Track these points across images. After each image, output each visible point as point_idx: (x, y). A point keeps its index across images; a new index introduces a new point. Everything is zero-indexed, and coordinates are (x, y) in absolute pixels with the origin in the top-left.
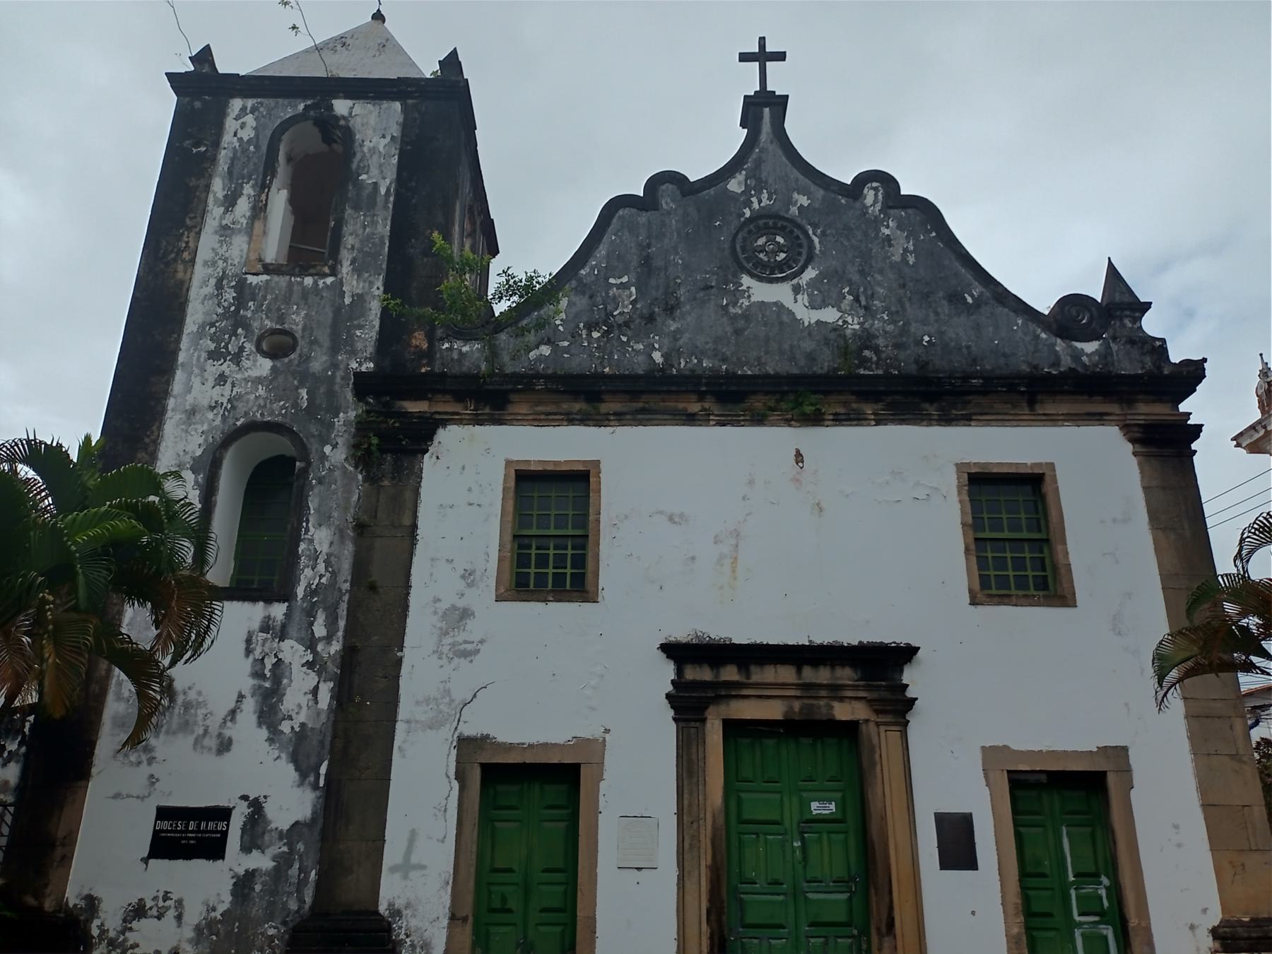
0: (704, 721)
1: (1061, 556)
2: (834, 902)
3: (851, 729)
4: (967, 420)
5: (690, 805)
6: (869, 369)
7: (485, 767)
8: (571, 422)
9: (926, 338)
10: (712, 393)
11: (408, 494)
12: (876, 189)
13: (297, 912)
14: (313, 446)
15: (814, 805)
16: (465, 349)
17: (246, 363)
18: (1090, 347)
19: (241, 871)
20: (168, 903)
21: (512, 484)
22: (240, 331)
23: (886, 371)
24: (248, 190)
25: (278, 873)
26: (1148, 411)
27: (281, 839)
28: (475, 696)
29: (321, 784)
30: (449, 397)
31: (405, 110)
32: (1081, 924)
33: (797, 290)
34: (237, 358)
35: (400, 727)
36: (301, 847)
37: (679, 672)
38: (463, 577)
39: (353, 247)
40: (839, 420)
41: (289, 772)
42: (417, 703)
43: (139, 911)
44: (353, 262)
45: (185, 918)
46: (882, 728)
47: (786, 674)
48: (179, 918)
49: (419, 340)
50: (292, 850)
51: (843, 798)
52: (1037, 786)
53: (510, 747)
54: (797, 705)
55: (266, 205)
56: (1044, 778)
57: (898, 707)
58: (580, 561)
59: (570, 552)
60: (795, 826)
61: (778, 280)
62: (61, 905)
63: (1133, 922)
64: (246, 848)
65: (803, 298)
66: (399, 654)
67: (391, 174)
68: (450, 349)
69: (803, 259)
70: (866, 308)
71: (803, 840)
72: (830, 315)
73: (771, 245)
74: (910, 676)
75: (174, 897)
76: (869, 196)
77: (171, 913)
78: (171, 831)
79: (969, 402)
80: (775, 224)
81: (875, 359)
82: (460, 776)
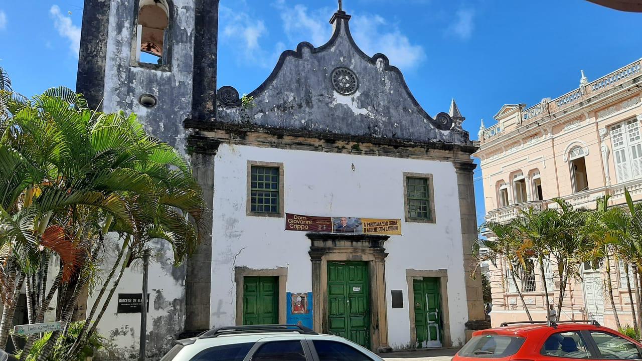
1: (432, 207)
2: (358, 321)
3: (367, 263)
7: (245, 277)
8: (272, 146)
9: (396, 124)
10: (324, 139)
11: (209, 172)
12: (381, 62)
13: (179, 331)
15: (354, 288)
16: (229, 111)
17: (135, 109)
18: (446, 133)
22: (131, 93)
23: (383, 136)
24: (127, 24)
25: (170, 318)
26: (463, 157)
29: (184, 284)
30: (223, 132)
32: (430, 324)
33: (353, 100)
34: (130, 105)
36: (178, 307)
37: (312, 244)
38: (234, 206)
39: (178, 59)
42: (219, 254)
44: (178, 66)
46: (377, 263)
47: (348, 243)
49: (209, 105)
50: (175, 309)
51: (363, 286)
52: (420, 281)
53: (254, 270)
55: (136, 33)
56: (422, 279)
57: (383, 255)
59: (271, 198)
60: (347, 295)
61: (346, 95)
63: (445, 322)
64: (157, 308)
65: (355, 103)
68: (223, 111)
69: (355, 89)
70: (376, 110)
71: (350, 300)
72: (364, 112)
74: (386, 245)
76: (379, 63)
78: (126, 303)
80: (346, 71)
81: (379, 130)
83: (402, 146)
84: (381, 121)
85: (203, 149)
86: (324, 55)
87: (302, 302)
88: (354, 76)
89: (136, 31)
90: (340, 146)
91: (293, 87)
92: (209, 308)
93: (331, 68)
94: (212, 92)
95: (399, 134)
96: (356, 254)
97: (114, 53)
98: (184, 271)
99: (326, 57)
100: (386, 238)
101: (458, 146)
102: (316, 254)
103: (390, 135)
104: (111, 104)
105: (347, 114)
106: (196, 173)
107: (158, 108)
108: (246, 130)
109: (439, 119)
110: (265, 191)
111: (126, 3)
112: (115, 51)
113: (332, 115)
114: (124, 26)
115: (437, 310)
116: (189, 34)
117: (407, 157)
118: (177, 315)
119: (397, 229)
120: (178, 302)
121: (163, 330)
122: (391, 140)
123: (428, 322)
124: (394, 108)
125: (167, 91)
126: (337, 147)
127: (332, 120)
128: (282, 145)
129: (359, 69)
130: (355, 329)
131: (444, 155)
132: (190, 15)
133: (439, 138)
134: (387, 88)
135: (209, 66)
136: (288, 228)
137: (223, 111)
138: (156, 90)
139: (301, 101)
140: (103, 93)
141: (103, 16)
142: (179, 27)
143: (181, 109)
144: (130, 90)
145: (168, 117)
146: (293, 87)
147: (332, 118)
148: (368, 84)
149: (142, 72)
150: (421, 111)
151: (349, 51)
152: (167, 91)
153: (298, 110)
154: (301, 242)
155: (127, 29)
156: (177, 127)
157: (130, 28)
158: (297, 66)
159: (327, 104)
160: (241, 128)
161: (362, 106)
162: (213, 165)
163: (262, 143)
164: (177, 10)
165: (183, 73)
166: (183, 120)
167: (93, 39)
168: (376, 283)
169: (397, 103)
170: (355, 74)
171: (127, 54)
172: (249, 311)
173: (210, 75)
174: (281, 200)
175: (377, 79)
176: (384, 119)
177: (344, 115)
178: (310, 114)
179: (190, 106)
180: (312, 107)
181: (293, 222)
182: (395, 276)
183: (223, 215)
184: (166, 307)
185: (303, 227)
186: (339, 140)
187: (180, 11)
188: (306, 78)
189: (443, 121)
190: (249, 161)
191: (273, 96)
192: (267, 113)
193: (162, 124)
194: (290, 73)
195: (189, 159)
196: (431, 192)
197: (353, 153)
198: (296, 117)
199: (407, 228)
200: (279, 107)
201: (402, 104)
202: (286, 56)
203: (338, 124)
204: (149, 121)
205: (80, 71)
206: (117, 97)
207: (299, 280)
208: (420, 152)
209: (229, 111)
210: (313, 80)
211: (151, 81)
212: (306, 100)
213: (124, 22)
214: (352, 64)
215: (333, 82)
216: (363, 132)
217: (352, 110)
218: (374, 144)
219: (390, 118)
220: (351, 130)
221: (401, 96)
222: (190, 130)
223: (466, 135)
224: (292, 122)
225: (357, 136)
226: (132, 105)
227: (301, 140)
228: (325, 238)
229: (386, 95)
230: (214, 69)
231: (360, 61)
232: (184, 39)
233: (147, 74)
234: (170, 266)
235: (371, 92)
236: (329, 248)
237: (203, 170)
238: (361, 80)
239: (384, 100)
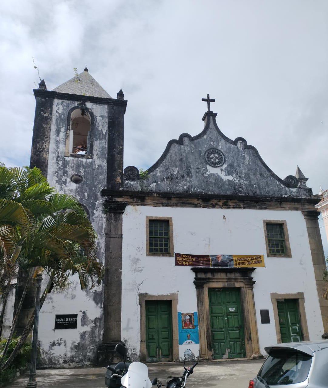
0: (203, 288)
3: (239, 289)
4: (265, 208)
5: (201, 310)
8: (163, 206)
9: (255, 186)
10: (202, 199)
11: (119, 225)
12: (241, 143)
13: (99, 342)
14: (90, 210)
17: (68, 184)
18: (294, 190)
19: (82, 332)
20: (62, 341)
21: (148, 223)
22: (65, 175)
24: (63, 130)
25: (93, 332)
26: (308, 207)
27: (92, 322)
28: (142, 282)
30: (128, 197)
31: (109, 109)
32: (292, 336)
33: (222, 170)
34: (65, 183)
35: (123, 291)
36: (98, 324)
37: (196, 275)
39: (97, 150)
40: (234, 207)
41: (93, 303)
43: (53, 344)
44: (97, 154)
45: (67, 345)
46: (247, 289)
47: (223, 275)
48: (65, 345)
49: (119, 180)
50: (96, 325)
51: (237, 307)
52: (282, 302)
53: (153, 296)
54: (226, 284)
55: (69, 135)
56: (283, 300)
57: (251, 283)
58: (167, 245)
59: (164, 242)
61: (217, 167)
64: (83, 325)
65: (223, 173)
66: (121, 271)
68: (128, 183)
69: (223, 162)
70: (240, 176)
71: (228, 318)
72: (230, 178)
73: (214, 157)
74: (254, 275)
75: (63, 339)
76: (240, 145)
77: (63, 344)
79: (266, 203)
80: (215, 151)
81: (242, 191)
82: (140, 304)
83: (261, 201)
84: (244, 184)
85: (115, 210)
86: (199, 141)
87: (190, 320)
88: (221, 154)
89: (69, 133)
90: (214, 203)
91: (177, 164)
92: (120, 325)
93: (204, 150)
94: (120, 171)
95: (258, 192)
96: (230, 283)
97: (54, 148)
98: (102, 297)
99: (201, 143)
100: (253, 270)
101: (304, 199)
102: (199, 284)
103: (251, 194)
104: (52, 182)
105: (218, 180)
106: (110, 227)
107: (84, 183)
108: (144, 195)
109: (288, 180)
110: (159, 239)
111: (62, 116)
112: (55, 147)
113: (206, 181)
114: (60, 131)
115: (298, 325)
116: (104, 134)
117: (265, 208)
118: (97, 329)
119: (260, 262)
120: (98, 320)
121: (87, 342)
122: (251, 197)
123: (292, 334)
124: (253, 174)
125: (89, 172)
126: (212, 204)
127: (207, 185)
128: (171, 205)
129: (225, 149)
130: (233, 340)
132: (105, 121)
134: (247, 161)
135: (118, 154)
136: (177, 264)
137: (128, 183)
138: (82, 171)
139: (184, 173)
140: (47, 175)
141: (47, 125)
142: (97, 129)
143: (99, 183)
144: (65, 173)
145: (90, 189)
146: (177, 164)
147: (207, 183)
148: (232, 158)
149: (73, 160)
150: (273, 175)
152: (89, 172)
153: (181, 179)
154: (187, 275)
155: (63, 133)
156: (96, 195)
157: (65, 132)
158: (180, 150)
159: (203, 174)
160: (141, 194)
162: (122, 220)
163: (156, 204)
164: (96, 118)
165: (101, 159)
166: (101, 190)
167: (40, 140)
168: (247, 305)
169: (255, 171)
170: (222, 152)
171: (63, 149)
172: (151, 326)
173: (119, 160)
174: (171, 243)
175: (239, 155)
176: (246, 182)
177: (215, 181)
178: (190, 182)
179: (105, 181)
180: (192, 177)
181: (181, 260)
182: (262, 298)
183: (130, 256)
184: (89, 324)
185: (188, 263)
186: (212, 199)
188: (187, 158)
189: (290, 182)
190: (147, 217)
191: (163, 171)
192: (159, 183)
193: (86, 194)
194: (175, 155)
195: (105, 217)
196: (286, 234)
197: (224, 207)
198: (180, 184)
199: (269, 261)
200: (167, 178)
201: (259, 172)
202: (172, 144)
203: (211, 188)
204: (78, 192)
205: (32, 161)
206: (56, 178)
207: (187, 303)
208: (275, 205)
209: (132, 183)
210: (191, 158)
211: (79, 166)
212: (187, 172)
213: (61, 129)
214: (220, 146)
215: (206, 159)
216: (231, 192)
217: (221, 178)
218: (239, 200)
219: (250, 181)
220: (221, 191)
221: (257, 165)
222: (106, 197)
223: (310, 191)
224: (177, 188)
225: (226, 195)
226: (66, 182)
228: (206, 271)
229: (246, 165)
230: (121, 155)
232: (101, 137)
233: (76, 161)
234: (92, 293)
235: (235, 164)
236: (209, 278)
237: (115, 224)
238: (227, 156)
239: (245, 169)
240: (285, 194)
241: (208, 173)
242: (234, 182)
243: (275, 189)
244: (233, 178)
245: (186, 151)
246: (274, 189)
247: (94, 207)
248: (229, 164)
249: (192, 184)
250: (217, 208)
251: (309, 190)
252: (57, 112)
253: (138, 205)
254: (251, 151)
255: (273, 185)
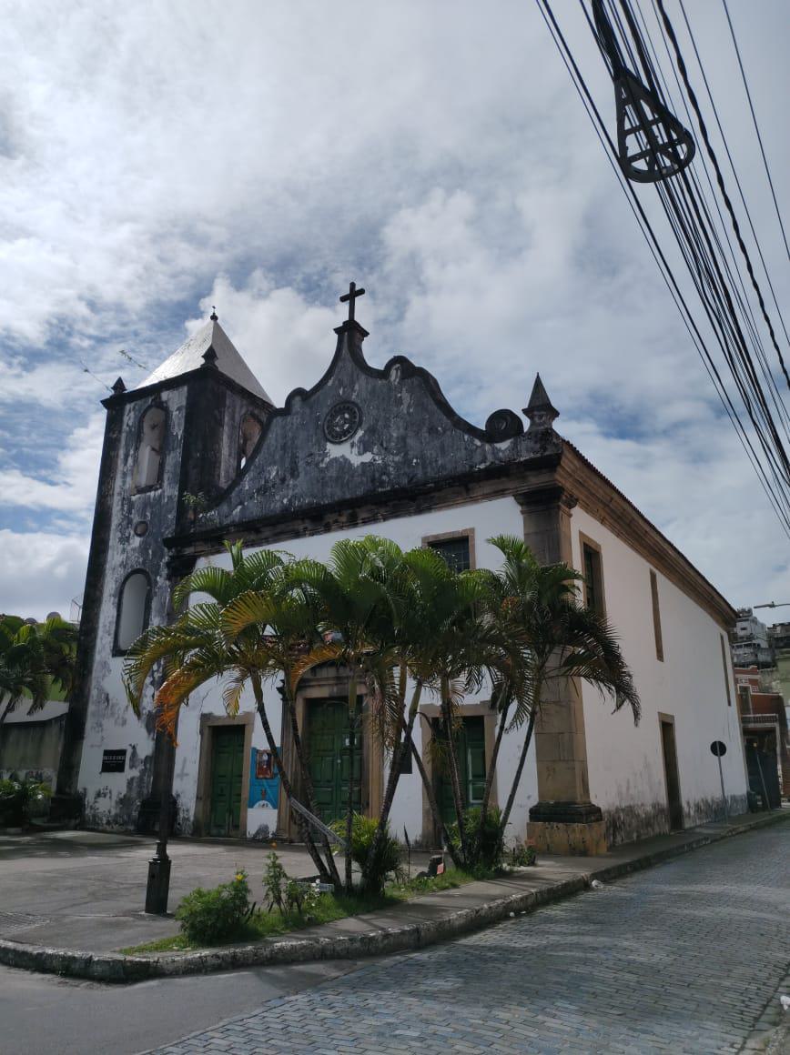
4: (429, 509)
6: (382, 487)
9: (415, 461)
12: (397, 369)
14: (153, 577)
17: (131, 541)
24: (132, 452)
26: (536, 481)
30: (201, 543)
33: (352, 446)
34: (128, 539)
62: (77, 792)
65: (355, 450)
67: (182, 428)
70: (386, 449)
72: (367, 457)
79: (432, 497)
91: (277, 457)
93: (326, 410)
95: (420, 474)
103: (405, 481)
127: (322, 486)
131: (501, 487)
133: (490, 458)
143: (167, 528)
144: (130, 521)
145: (156, 541)
148: (374, 412)
151: (353, 372)
158: (284, 427)
159: (317, 465)
161: (365, 450)
170: (356, 405)
176: (397, 459)
180: (298, 476)
187: (174, 413)
189: (503, 423)
192: (246, 504)
193: (150, 552)
201: (427, 425)
211: (146, 504)
218: (376, 504)
227: (280, 528)
231: (367, 383)
235: (379, 423)
240: (481, 463)
241: (327, 460)
242: (374, 465)
243: (459, 455)
244: (372, 456)
245: (295, 424)
246: (455, 458)
247: (157, 573)
248: (368, 428)
249: (296, 491)
250: (335, 530)
251: (543, 434)
252: (128, 425)
253: (213, 554)
254: (416, 380)
255: (455, 447)
